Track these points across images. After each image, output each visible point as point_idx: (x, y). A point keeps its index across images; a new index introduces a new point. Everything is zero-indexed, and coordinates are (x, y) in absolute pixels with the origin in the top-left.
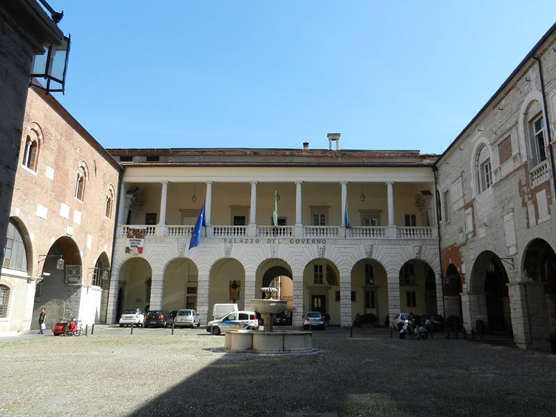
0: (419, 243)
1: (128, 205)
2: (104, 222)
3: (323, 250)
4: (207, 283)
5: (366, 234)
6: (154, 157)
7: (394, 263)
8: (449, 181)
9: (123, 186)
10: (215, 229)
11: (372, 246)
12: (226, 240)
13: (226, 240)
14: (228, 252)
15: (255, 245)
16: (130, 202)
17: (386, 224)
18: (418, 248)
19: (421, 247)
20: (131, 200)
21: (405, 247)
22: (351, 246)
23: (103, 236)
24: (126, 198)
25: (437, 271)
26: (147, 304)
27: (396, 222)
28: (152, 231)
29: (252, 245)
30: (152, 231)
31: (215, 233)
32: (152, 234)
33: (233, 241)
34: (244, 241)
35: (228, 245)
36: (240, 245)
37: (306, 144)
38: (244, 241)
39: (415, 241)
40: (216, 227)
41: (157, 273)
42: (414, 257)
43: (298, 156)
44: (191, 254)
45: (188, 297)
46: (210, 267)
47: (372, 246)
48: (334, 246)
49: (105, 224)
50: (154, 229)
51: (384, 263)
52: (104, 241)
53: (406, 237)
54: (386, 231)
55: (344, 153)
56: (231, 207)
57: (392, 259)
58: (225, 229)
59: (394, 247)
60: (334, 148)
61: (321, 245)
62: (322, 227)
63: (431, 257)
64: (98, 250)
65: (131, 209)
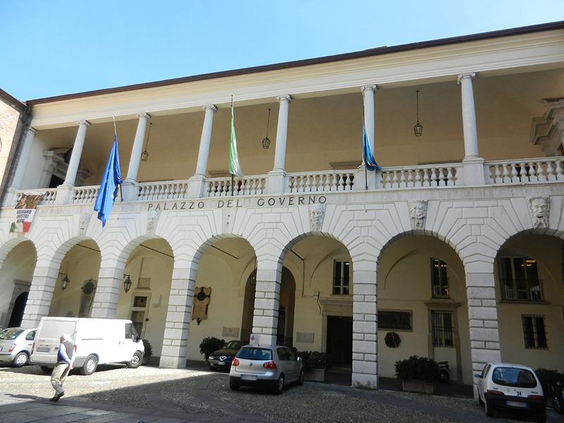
0: (546, 192)
3: (319, 217)
11: (426, 203)
12: (150, 205)
13: (150, 205)
15: (197, 212)
16: (50, 161)
18: (542, 203)
20: (53, 158)
21: (506, 203)
22: (380, 206)
29: (193, 212)
33: (162, 207)
34: (179, 206)
35: (153, 213)
36: (174, 213)
38: (179, 206)
39: (533, 189)
42: (530, 224)
44: (94, 232)
47: (426, 203)
48: (344, 207)
51: (453, 241)
53: (507, 181)
58: (146, 188)
59: (476, 204)
61: (316, 207)
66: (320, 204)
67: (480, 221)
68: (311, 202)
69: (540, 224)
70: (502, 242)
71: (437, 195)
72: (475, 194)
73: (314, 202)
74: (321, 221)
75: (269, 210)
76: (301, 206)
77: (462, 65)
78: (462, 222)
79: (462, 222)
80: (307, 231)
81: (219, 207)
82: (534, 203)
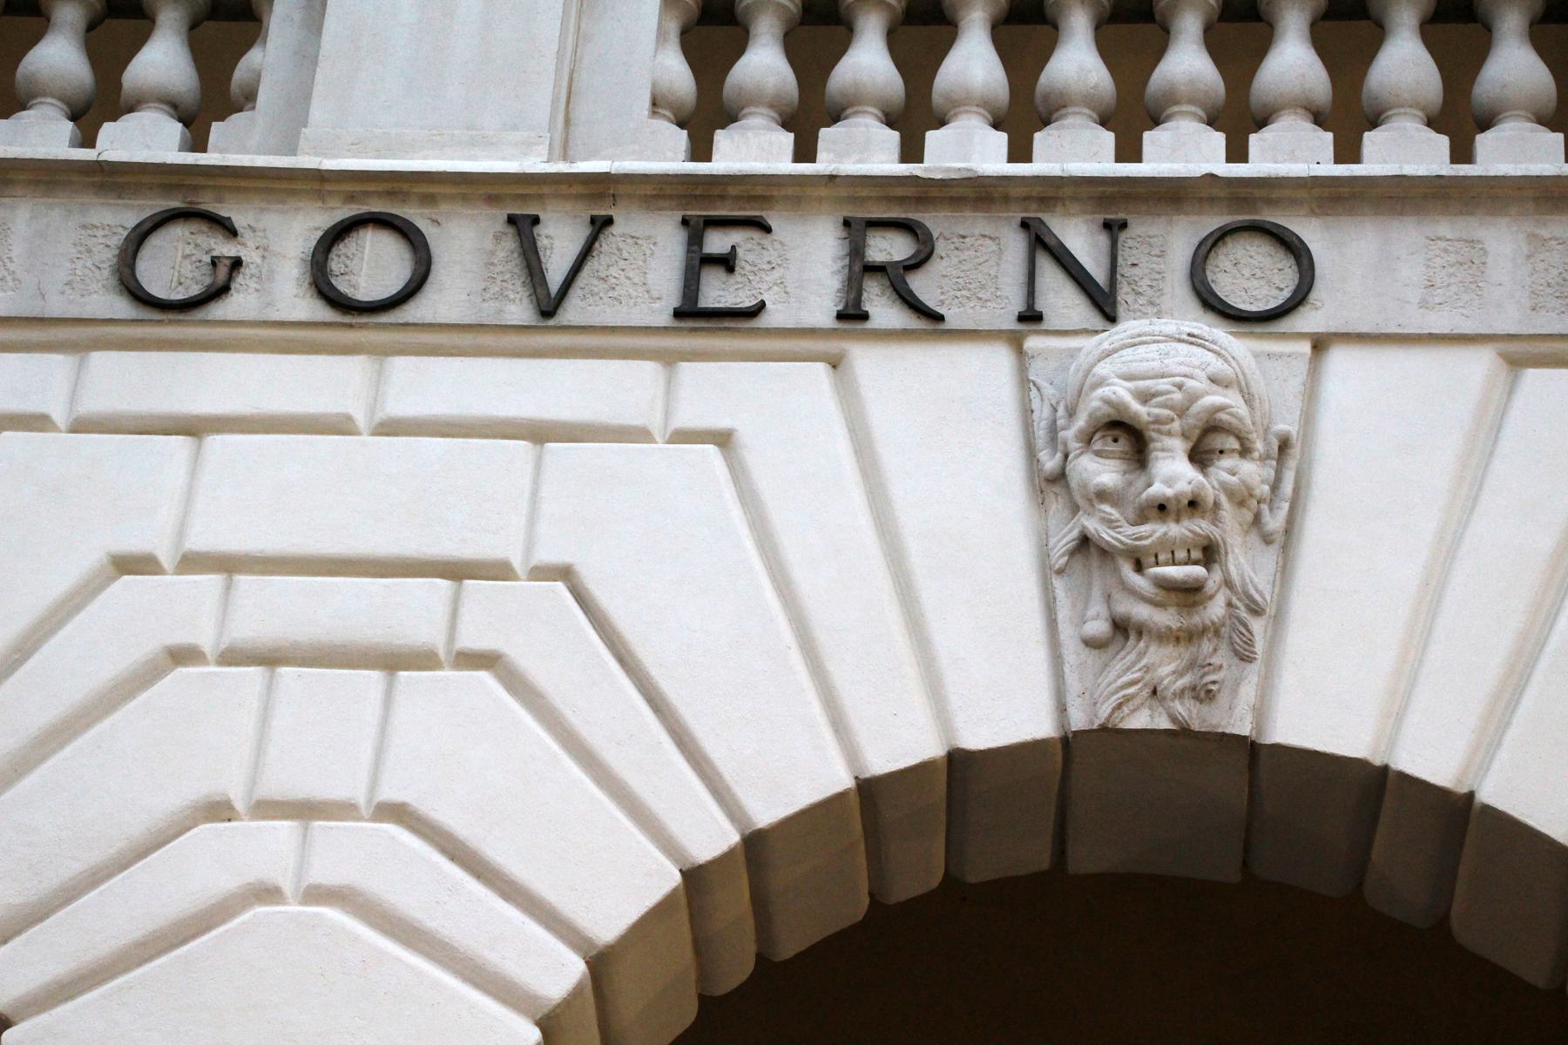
68: (1061, 300)
73: (1104, 303)
74: (1247, 563)
76: (893, 373)
80: (1009, 706)
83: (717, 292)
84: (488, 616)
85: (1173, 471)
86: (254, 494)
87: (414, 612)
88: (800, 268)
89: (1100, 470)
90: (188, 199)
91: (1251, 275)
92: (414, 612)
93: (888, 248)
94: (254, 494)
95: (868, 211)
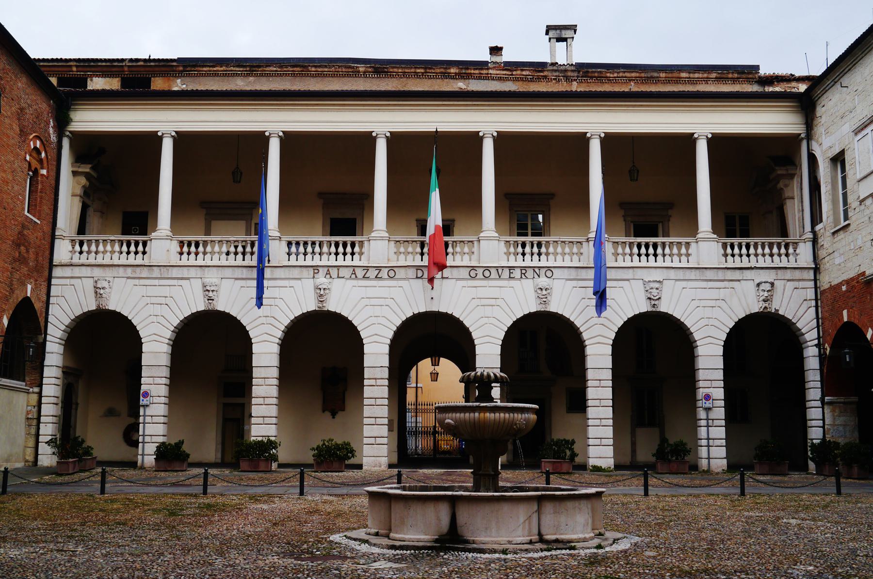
1: (79, 191)
2: (24, 227)
3: (543, 293)
4: (275, 372)
5: (647, 255)
6: (139, 80)
7: (711, 322)
8: (847, 128)
9: (66, 143)
10: (289, 244)
14: (321, 294)
17: (692, 228)
19: (772, 284)
23: (22, 260)
24: (75, 173)
25: (811, 336)
26: (132, 420)
27: (715, 229)
28: (140, 248)
30: (140, 248)
31: (289, 254)
32: (140, 255)
35: (321, 280)
37: (496, 50)
40: (293, 239)
41: (156, 353)
43: (479, 78)
45: (225, 405)
46: (279, 334)
49: (25, 232)
50: (145, 244)
52: (25, 270)
54: (693, 245)
55: (585, 70)
56: (321, 195)
57: (708, 312)
60: (561, 60)
62: (536, 239)
63: (797, 306)
64: (12, 291)
65: (88, 202)
66: (546, 279)
67: (713, 303)
68: (536, 276)
69: (766, 308)
70: (731, 324)
71: (672, 274)
72: (710, 275)
74: (549, 298)
75: (485, 283)
76: (524, 281)
77: (702, 123)
78: (696, 303)
79: (696, 303)
81: (417, 277)
82: (761, 287)
83: (512, 276)
84: (499, 302)
85: (544, 292)
86: (482, 292)
87: (493, 302)
88: (517, 273)
89: (539, 291)
90: (473, 268)
91: (549, 274)
92: (493, 302)
93: (524, 272)
94: (482, 292)
95: (522, 268)
